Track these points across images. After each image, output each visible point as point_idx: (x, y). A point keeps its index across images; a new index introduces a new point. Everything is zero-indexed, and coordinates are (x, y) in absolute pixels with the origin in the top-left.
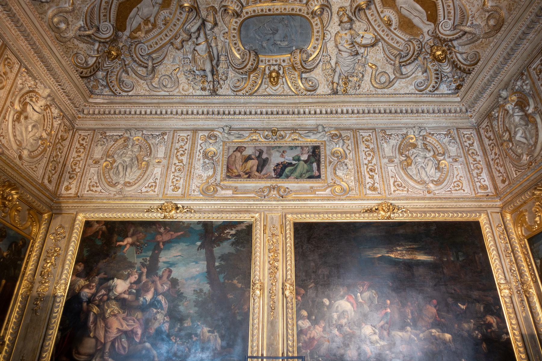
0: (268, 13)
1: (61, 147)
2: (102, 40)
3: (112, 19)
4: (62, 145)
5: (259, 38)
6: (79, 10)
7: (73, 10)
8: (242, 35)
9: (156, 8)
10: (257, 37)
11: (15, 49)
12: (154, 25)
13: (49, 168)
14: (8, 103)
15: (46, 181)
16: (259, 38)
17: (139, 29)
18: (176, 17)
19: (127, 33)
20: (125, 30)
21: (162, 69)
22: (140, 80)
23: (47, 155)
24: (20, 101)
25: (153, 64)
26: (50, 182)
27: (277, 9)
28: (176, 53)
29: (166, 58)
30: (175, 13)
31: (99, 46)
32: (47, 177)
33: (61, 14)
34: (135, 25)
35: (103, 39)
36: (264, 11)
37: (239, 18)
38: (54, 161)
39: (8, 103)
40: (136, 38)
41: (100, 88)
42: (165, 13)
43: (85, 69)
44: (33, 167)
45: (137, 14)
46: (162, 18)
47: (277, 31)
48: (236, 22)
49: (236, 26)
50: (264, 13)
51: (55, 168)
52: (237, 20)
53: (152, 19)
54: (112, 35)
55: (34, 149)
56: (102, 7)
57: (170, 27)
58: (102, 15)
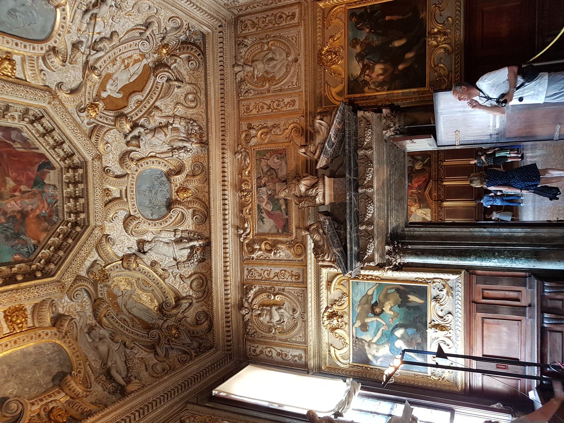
0: (19, 42)
1: (261, 22)
2: (170, 71)
3: (152, 81)
4: (259, 21)
5: (34, 12)
6: (173, 101)
7: (178, 103)
8: (52, 22)
9: (115, 76)
10: (35, 14)
11: (235, 111)
12: (123, 61)
13: (284, 23)
14: (270, 94)
15: (296, 20)
16: (34, 12)
17: (136, 61)
18: (105, 65)
19: (145, 62)
20: (145, 65)
21: (140, 20)
22: (162, 19)
23: (276, 33)
24: (263, 86)
25: (145, 30)
26: (293, 16)
27: (8, 43)
28: (119, 29)
29: (130, 28)
30: (104, 68)
31: (172, 64)
32: (292, 22)
33: (186, 105)
34: (137, 66)
35: (169, 73)
36: (23, 45)
37: (51, 45)
38: (276, 22)
39: (270, 94)
40: (140, 55)
41: (192, 30)
42: (111, 70)
43: (195, 56)
44: (293, 41)
45: (131, 76)
46: (115, 66)
47: (9, 12)
48: (55, 42)
49: (55, 37)
50: (24, 43)
51: (281, 17)
52: (55, 45)
53: (123, 67)
54: (161, 72)
55: (281, 50)
56: (157, 95)
57: (114, 57)
58: (159, 89)
